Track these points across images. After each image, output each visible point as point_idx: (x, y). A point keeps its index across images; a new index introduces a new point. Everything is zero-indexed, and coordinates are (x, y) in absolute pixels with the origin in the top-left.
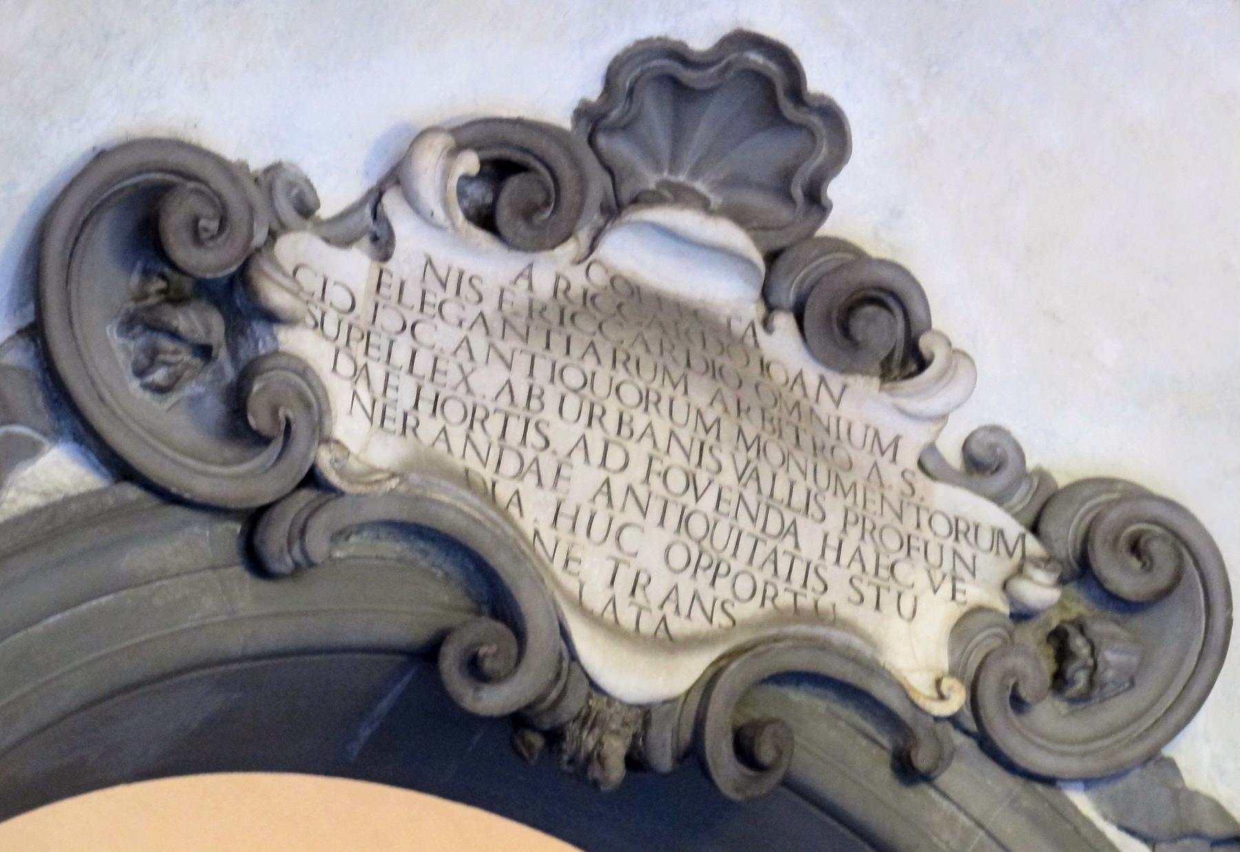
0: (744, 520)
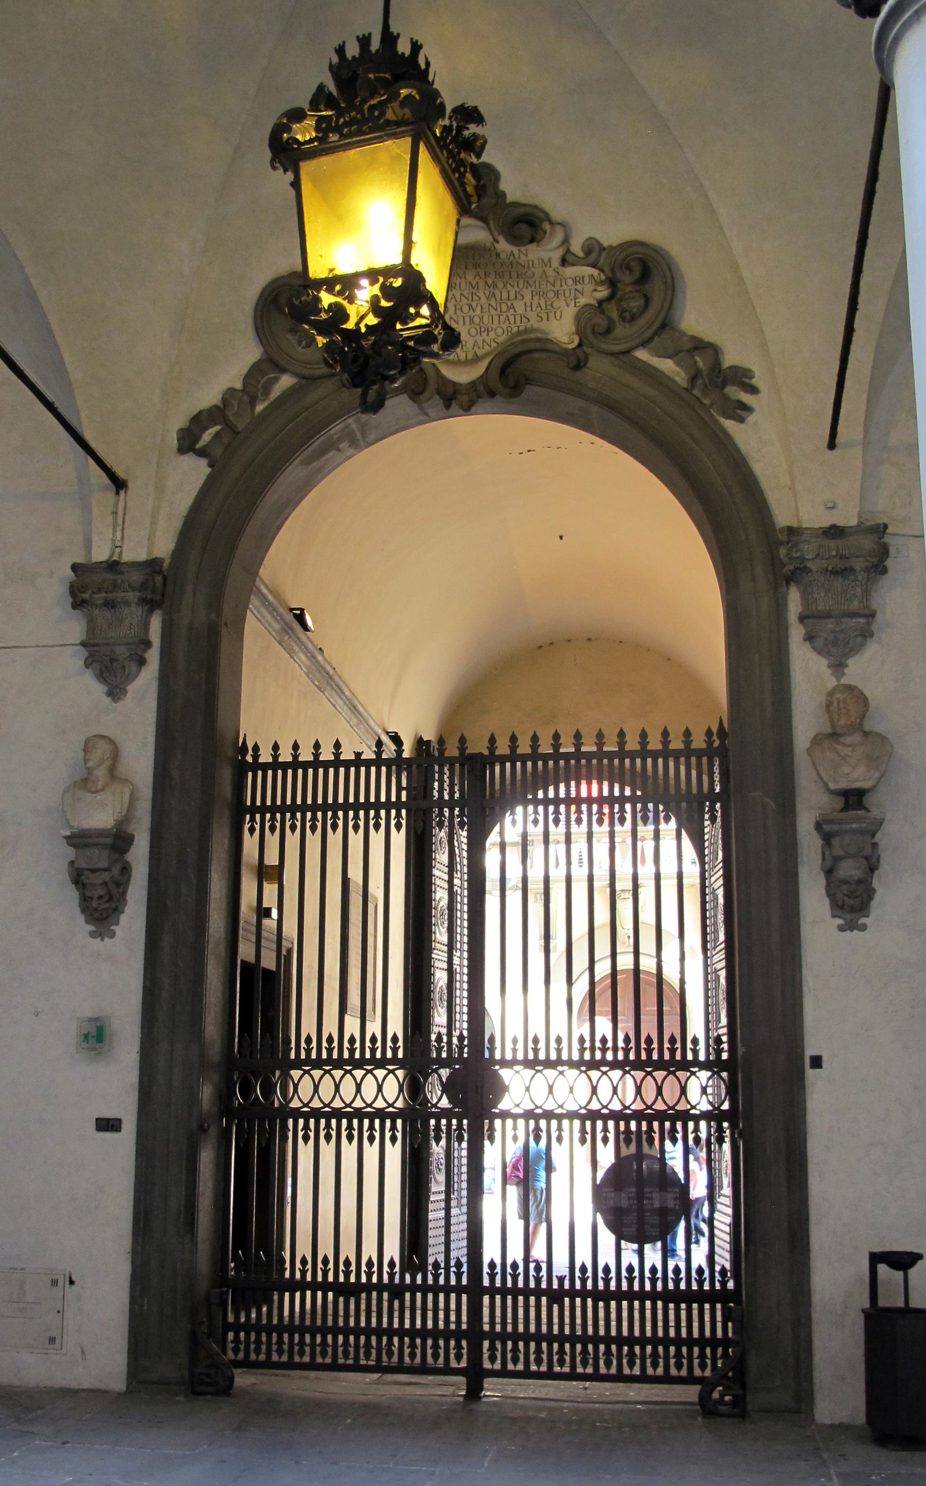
0: (493, 312)
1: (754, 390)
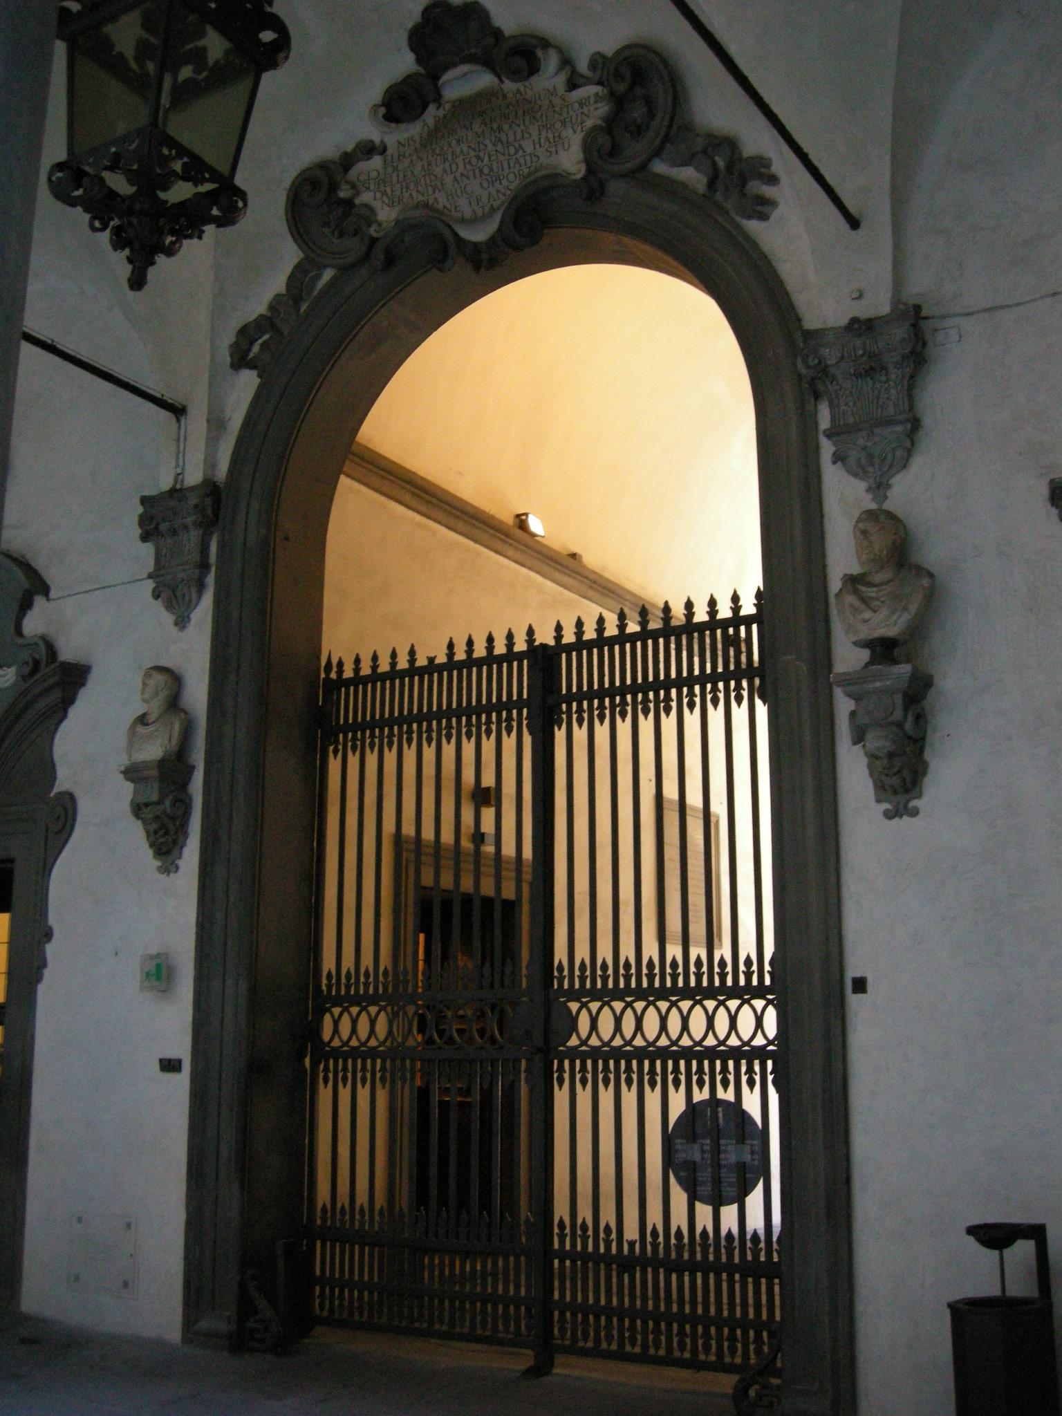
0: (502, 158)
1: (773, 180)
